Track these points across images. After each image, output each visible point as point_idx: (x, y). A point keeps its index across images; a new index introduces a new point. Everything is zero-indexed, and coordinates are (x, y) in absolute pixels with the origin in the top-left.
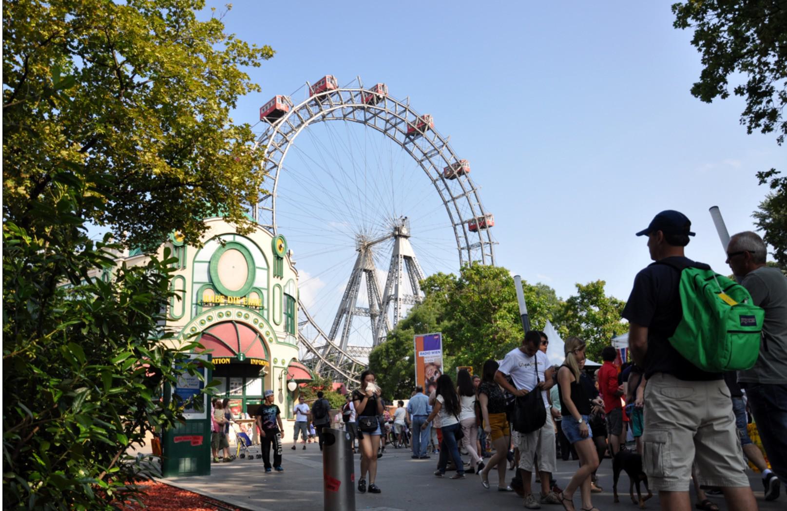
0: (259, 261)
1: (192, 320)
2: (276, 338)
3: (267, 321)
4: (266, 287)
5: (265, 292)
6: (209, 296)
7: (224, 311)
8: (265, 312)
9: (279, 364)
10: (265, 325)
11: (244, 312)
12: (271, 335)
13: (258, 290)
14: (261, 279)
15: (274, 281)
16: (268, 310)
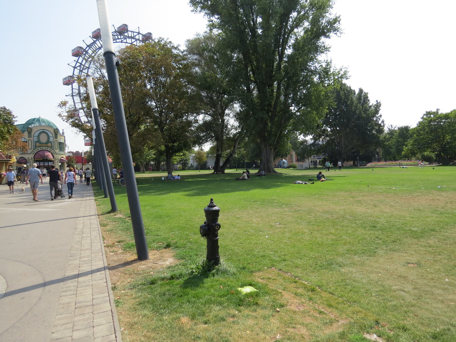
0: (50, 135)
1: (34, 150)
2: (56, 153)
3: (53, 150)
4: (53, 141)
5: (52, 143)
6: (38, 144)
7: (42, 148)
8: (53, 147)
9: (57, 159)
10: (53, 150)
11: (47, 148)
12: (54, 153)
13: (51, 142)
14: (51, 139)
15: (55, 140)
16: (53, 147)
